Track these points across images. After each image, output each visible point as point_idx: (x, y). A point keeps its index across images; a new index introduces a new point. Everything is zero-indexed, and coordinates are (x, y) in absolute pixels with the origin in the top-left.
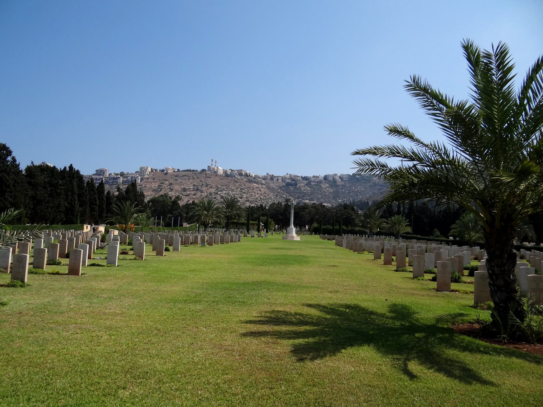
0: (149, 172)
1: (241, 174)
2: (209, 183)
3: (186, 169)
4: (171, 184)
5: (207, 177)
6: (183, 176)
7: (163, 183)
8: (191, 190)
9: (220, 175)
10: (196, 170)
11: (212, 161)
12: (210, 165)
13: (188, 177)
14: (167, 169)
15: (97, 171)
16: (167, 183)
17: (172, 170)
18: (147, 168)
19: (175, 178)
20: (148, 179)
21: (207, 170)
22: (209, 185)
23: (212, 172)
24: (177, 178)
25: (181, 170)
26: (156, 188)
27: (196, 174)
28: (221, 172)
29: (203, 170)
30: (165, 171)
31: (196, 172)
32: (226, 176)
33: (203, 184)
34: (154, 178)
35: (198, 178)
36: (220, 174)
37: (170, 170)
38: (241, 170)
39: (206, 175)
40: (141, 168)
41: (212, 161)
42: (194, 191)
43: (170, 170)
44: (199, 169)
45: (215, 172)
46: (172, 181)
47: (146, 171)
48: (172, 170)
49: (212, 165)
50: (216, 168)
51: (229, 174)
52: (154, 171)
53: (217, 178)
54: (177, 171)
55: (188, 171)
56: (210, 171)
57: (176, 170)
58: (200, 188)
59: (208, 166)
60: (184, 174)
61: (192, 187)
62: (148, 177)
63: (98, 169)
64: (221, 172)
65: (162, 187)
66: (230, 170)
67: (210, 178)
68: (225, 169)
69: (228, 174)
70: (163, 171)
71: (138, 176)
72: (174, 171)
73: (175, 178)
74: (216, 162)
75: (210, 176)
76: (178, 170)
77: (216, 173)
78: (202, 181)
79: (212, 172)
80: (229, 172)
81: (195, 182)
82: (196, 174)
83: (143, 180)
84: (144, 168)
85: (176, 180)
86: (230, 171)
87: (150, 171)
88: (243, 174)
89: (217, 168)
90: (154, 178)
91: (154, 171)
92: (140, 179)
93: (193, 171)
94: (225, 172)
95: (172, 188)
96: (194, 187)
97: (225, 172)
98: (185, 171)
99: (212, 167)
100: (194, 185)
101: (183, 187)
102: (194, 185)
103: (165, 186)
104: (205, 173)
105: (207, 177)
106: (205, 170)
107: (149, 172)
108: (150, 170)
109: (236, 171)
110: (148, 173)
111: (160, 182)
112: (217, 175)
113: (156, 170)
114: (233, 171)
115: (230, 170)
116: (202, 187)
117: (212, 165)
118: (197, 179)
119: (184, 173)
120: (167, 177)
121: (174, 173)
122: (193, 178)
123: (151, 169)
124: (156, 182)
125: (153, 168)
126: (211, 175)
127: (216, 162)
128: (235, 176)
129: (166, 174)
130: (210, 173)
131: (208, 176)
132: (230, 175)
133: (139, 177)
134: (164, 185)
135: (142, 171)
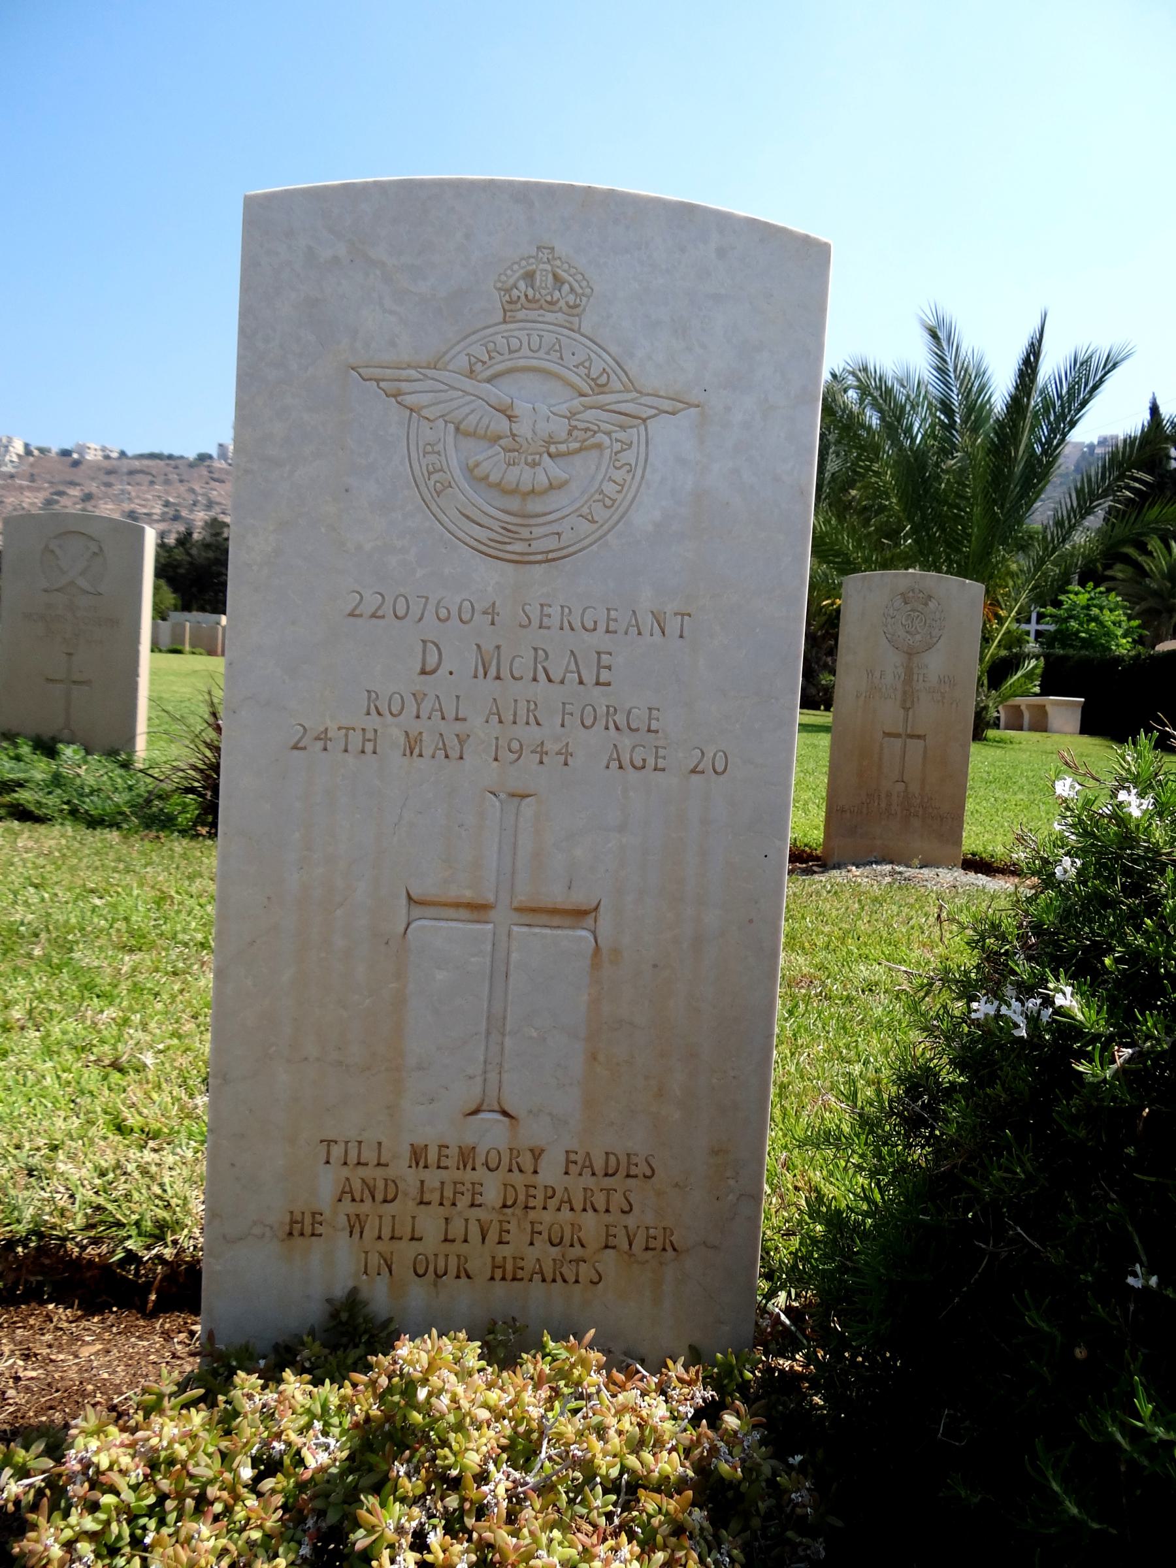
0: (19, 456)
2: (218, 499)
3: (146, 450)
4: (88, 497)
6: (131, 473)
7: (61, 494)
8: (155, 517)
10: (182, 457)
13: (150, 478)
14: (82, 449)
16: (75, 492)
17: (100, 453)
18: (10, 440)
19: (106, 479)
20: (12, 476)
22: (219, 504)
24: (111, 479)
25: (130, 453)
27: (176, 467)
29: (203, 458)
30: (75, 456)
31: (179, 462)
35: (181, 481)
37: (92, 452)
39: (210, 472)
42: (163, 520)
43: (92, 452)
44: (191, 455)
46: (93, 487)
48: (100, 453)
52: (36, 453)
54: (119, 458)
55: (152, 456)
57: (115, 455)
58: (184, 513)
59: (221, 445)
61: (158, 510)
62: (13, 470)
67: (223, 482)
70: (66, 453)
72: (107, 457)
73: (106, 479)
75: (223, 477)
76: (123, 454)
78: (192, 491)
81: (167, 493)
82: (176, 467)
85: (109, 485)
87: (21, 451)
90: (32, 478)
91: (36, 453)
93: (170, 457)
96: (166, 509)
98: (141, 457)
100: (167, 504)
101: (127, 507)
102: (167, 504)
103: (69, 503)
106: (210, 457)
107: (19, 456)
108: (18, 447)
110: (15, 459)
111: (52, 490)
116: (191, 511)
118: (179, 484)
119: (137, 464)
120: (78, 474)
121: (106, 463)
122: (167, 482)
123: (27, 446)
124: (38, 489)
125: (35, 443)
126: (227, 472)
129: (76, 464)
131: (215, 476)
134: (64, 501)
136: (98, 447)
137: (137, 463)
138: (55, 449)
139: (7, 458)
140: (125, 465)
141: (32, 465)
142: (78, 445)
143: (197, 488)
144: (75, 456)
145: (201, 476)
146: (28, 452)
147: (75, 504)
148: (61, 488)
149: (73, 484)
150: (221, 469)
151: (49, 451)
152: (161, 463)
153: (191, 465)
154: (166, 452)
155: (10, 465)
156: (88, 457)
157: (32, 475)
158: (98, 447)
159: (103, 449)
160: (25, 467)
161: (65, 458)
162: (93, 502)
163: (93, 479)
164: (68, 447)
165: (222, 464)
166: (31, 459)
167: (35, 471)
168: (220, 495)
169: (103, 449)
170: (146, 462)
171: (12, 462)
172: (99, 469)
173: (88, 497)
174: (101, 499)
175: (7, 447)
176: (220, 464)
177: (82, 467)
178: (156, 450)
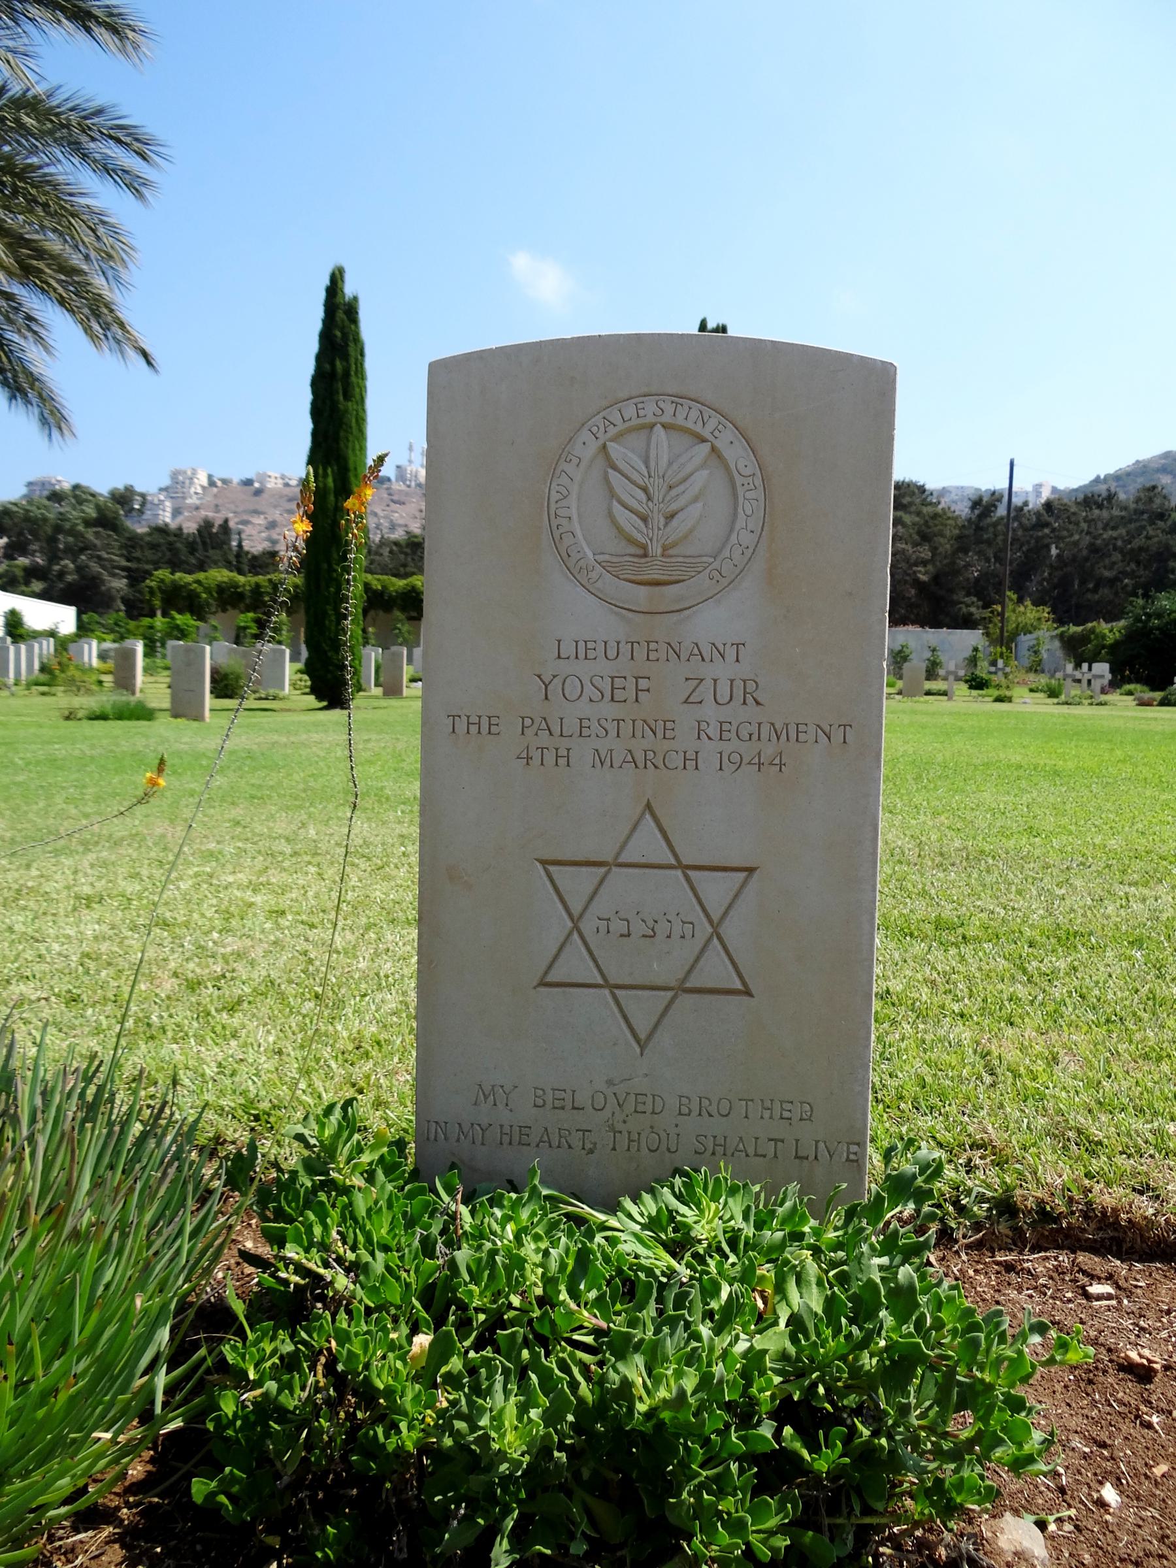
0: (203, 488)
2: (401, 522)
4: (272, 525)
5: (393, 501)
11: (411, 448)
14: (263, 477)
15: (30, 484)
16: (259, 521)
18: (194, 472)
20: (197, 508)
21: (393, 478)
23: (409, 486)
30: (257, 485)
37: (273, 480)
39: (390, 494)
40: (175, 475)
41: (411, 448)
43: (273, 480)
46: (276, 515)
47: (192, 483)
48: (280, 481)
49: (410, 461)
52: (219, 483)
56: (404, 482)
59: (398, 467)
62: (198, 502)
63: (32, 479)
70: (248, 483)
71: (162, 497)
72: (287, 485)
75: (403, 499)
79: (409, 486)
83: (180, 513)
84: (185, 472)
87: (205, 482)
92: (169, 509)
95: (275, 537)
99: (409, 469)
103: (254, 532)
104: (388, 489)
105: (393, 501)
106: (389, 480)
107: (203, 488)
110: (199, 490)
113: (224, 481)
117: (410, 461)
120: (262, 502)
123: (210, 477)
125: (218, 474)
126: (407, 494)
129: (258, 492)
130: (401, 486)
131: (395, 498)
133: (168, 504)
135: (177, 486)
136: (278, 475)
138: (236, 480)
139: (192, 490)
141: (215, 496)
142: (258, 474)
144: (257, 485)
145: (381, 499)
146: (212, 483)
147: (260, 532)
148: (245, 517)
149: (257, 512)
150: (400, 491)
155: (195, 497)
156: (269, 486)
157: (217, 506)
158: (278, 475)
159: (283, 477)
160: (209, 498)
162: (278, 530)
163: (275, 507)
164: (250, 475)
165: (401, 486)
166: (215, 490)
167: (220, 502)
168: (402, 517)
171: (196, 493)
172: (281, 497)
174: (285, 526)
175: (191, 479)
176: (397, 486)
177: (265, 496)
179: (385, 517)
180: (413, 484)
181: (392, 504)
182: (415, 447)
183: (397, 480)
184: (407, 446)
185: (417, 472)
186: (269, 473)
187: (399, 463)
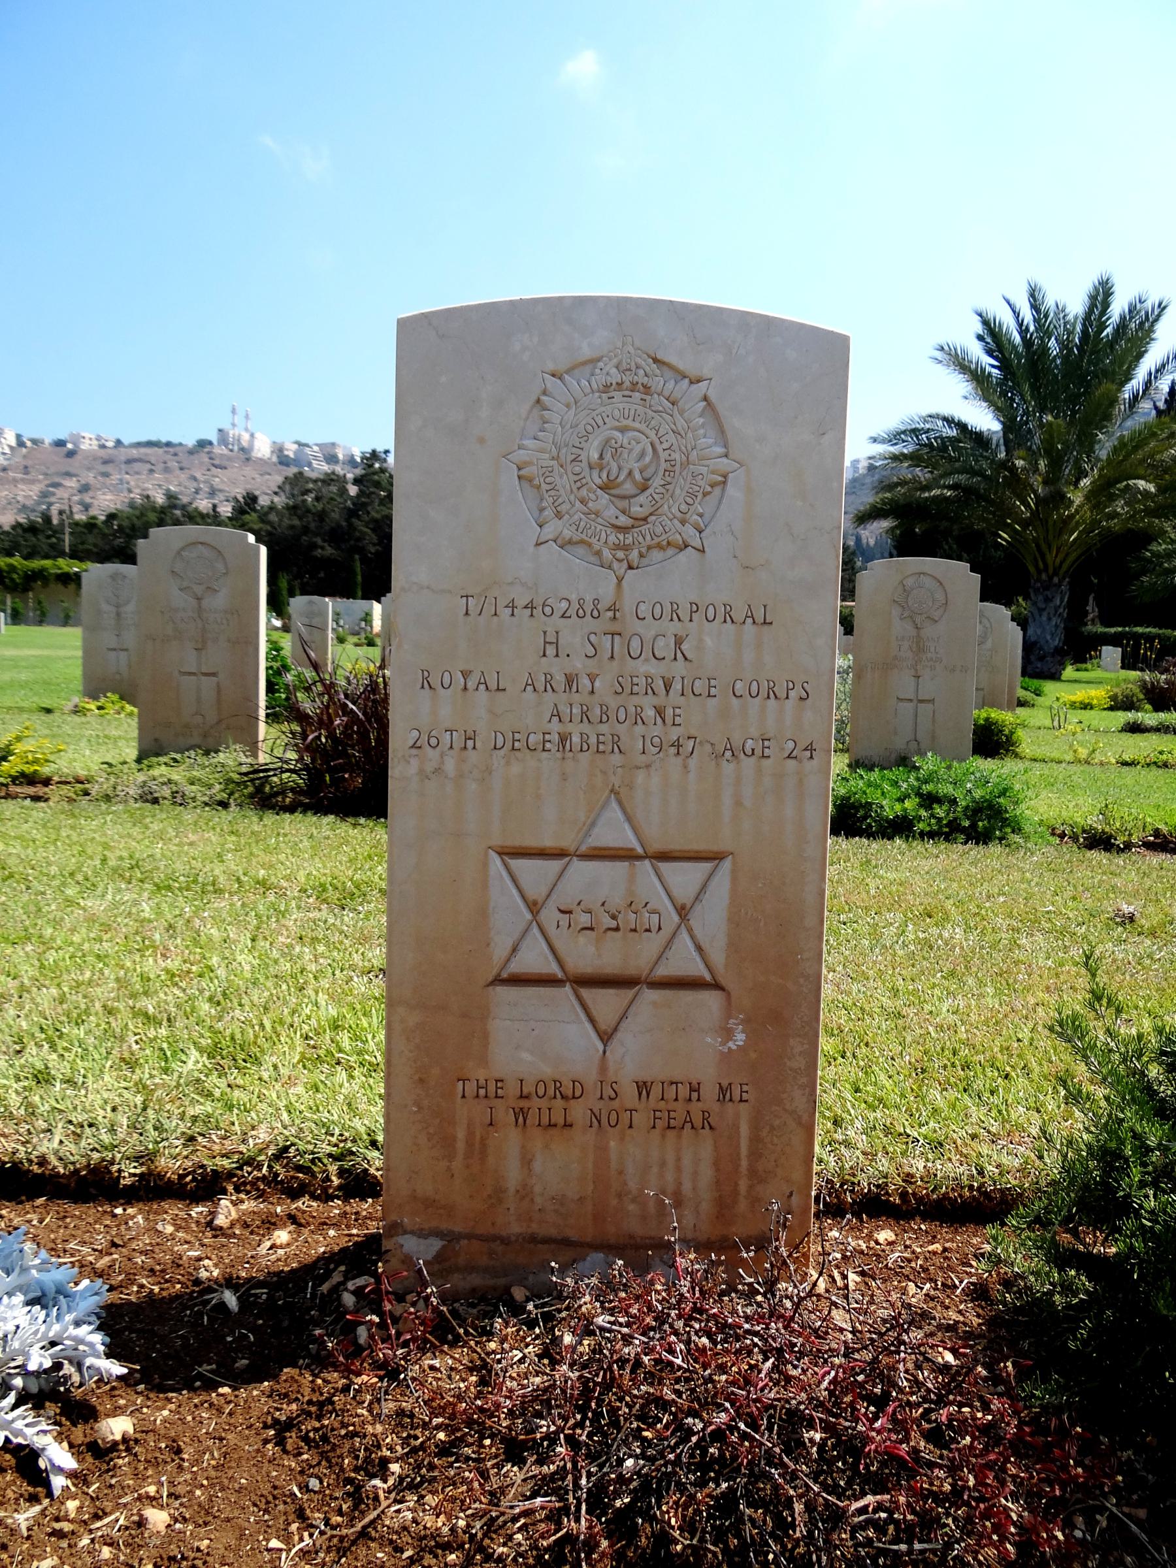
0: (11, 447)
1: (331, 459)
2: (221, 487)
3: (144, 438)
4: (85, 488)
5: (213, 465)
6: (129, 462)
7: (56, 485)
9: (261, 459)
10: (180, 444)
11: (234, 411)
12: (226, 426)
13: (149, 466)
14: (77, 438)
16: (72, 483)
19: (103, 468)
21: (215, 442)
22: (220, 491)
23: (231, 450)
24: (109, 468)
25: (126, 442)
26: (29, 503)
27: (175, 455)
28: (263, 449)
29: (203, 444)
30: (70, 446)
31: (178, 449)
32: (281, 463)
33: (201, 489)
34: (26, 470)
35: (181, 469)
36: (259, 455)
37: (87, 441)
38: (333, 444)
39: (211, 458)
41: (234, 411)
43: (87, 441)
44: (190, 442)
45: (242, 449)
46: (90, 477)
48: (95, 442)
49: (234, 425)
50: (246, 437)
51: (292, 455)
52: (29, 444)
53: (248, 471)
55: (150, 444)
57: (110, 444)
59: (220, 430)
60: (136, 456)
64: (263, 449)
65: (53, 499)
66: (297, 443)
68: (279, 441)
69: (287, 456)
70: (60, 443)
72: (103, 447)
73: (103, 468)
74: (247, 417)
75: (225, 463)
76: (119, 443)
77: (245, 453)
78: (195, 479)
79: (231, 450)
80: (291, 450)
81: (170, 483)
82: (175, 455)
85: (106, 475)
86: (295, 446)
87: (13, 443)
88: (341, 456)
89: (252, 435)
90: (26, 470)
91: (29, 444)
93: (168, 444)
94: (279, 450)
95: (88, 500)
97: (279, 450)
98: (139, 445)
99: (231, 432)
104: (209, 453)
105: (213, 465)
106: (210, 443)
107: (11, 447)
109: (316, 448)
110: (7, 450)
112: (248, 459)
113: (35, 442)
114: (307, 445)
115: (297, 443)
118: (178, 472)
119: (134, 452)
120: (74, 464)
121: (102, 453)
122: (167, 470)
123: (18, 437)
124: (33, 482)
126: (229, 459)
127: (247, 417)
128: (310, 465)
129: (71, 454)
131: (217, 462)
132: (294, 460)
134: (60, 493)
136: (93, 436)
137: (134, 451)
138: (48, 441)
140: (123, 454)
141: (25, 457)
142: (72, 435)
143: (198, 475)
144: (70, 446)
145: (202, 463)
146: (21, 444)
148: (57, 480)
149: (68, 474)
151: (43, 442)
152: (160, 451)
153: (191, 452)
154: (164, 440)
156: (82, 447)
157: (26, 467)
158: (93, 436)
159: (98, 438)
161: (59, 448)
162: (91, 493)
163: (89, 469)
164: (62, 437)
166: (24, 450)
167: (29, 463)
169: (98, 438)
170: (143, 450)
172: (95, 459)
173: (85, 488)
174: (99, 489)
176: (219, 450)
177: (78, 457)
178: (154, 438)
179: (205, 482)
180: (236, 448)
181: (213, 469)
182: (237, 411)
183: (219, 444)
184: (230, 409)
185: (239, 436)
186: (83, 434)
187: (221, 427)
